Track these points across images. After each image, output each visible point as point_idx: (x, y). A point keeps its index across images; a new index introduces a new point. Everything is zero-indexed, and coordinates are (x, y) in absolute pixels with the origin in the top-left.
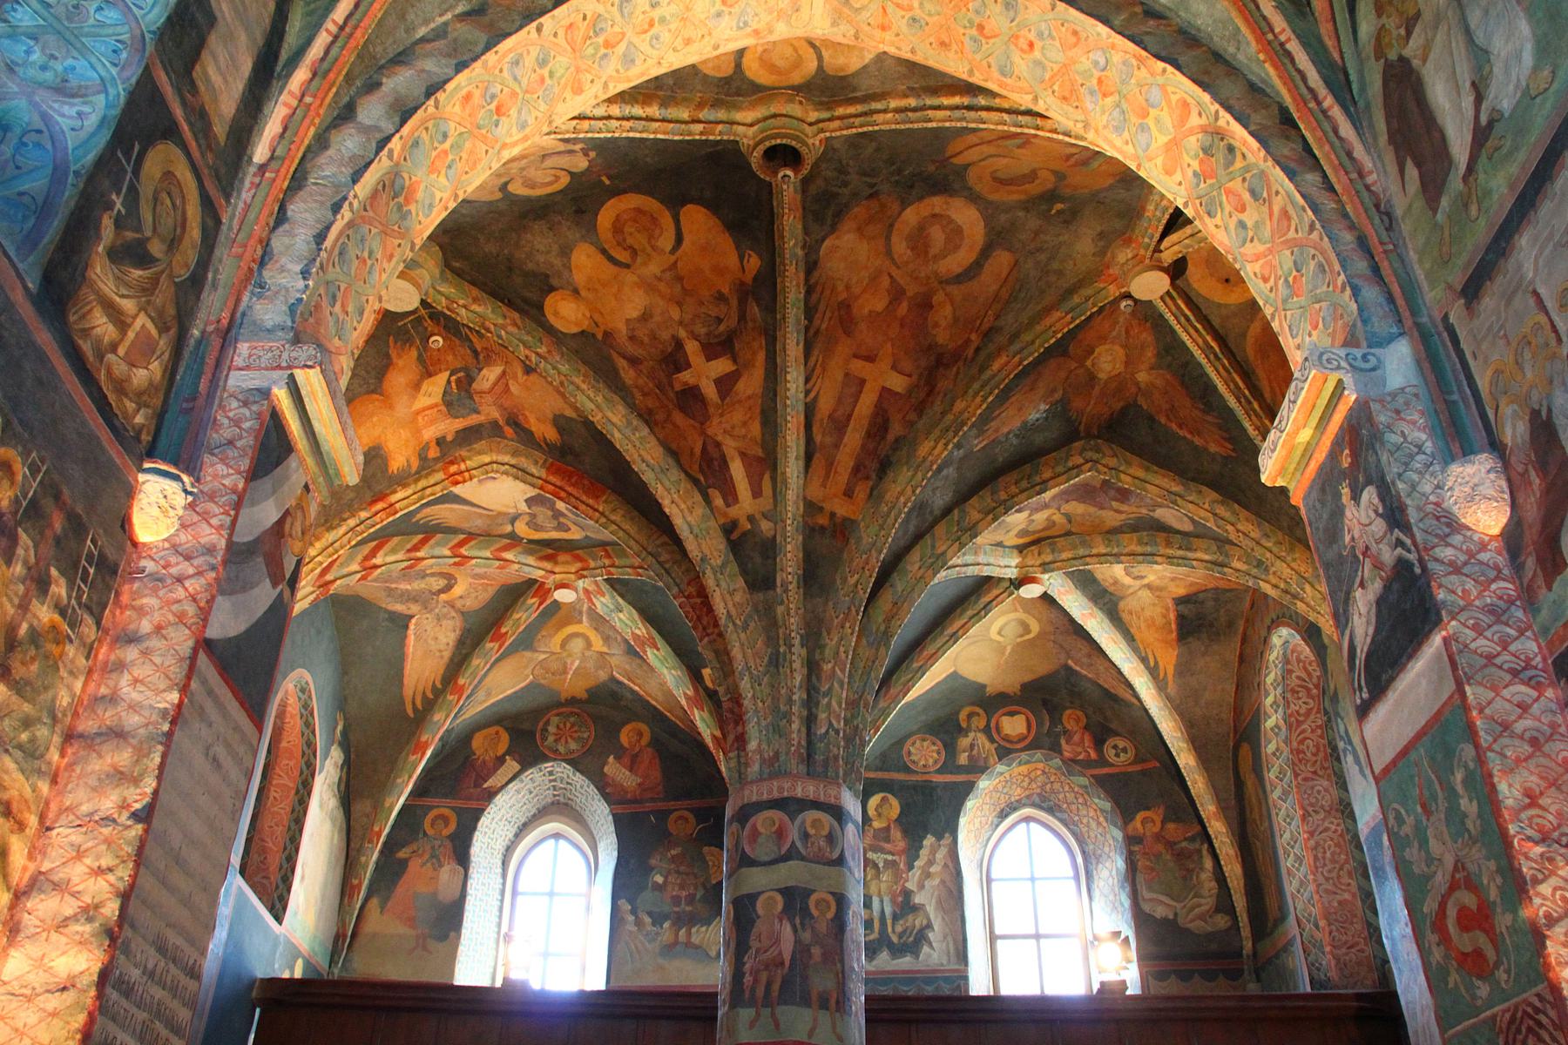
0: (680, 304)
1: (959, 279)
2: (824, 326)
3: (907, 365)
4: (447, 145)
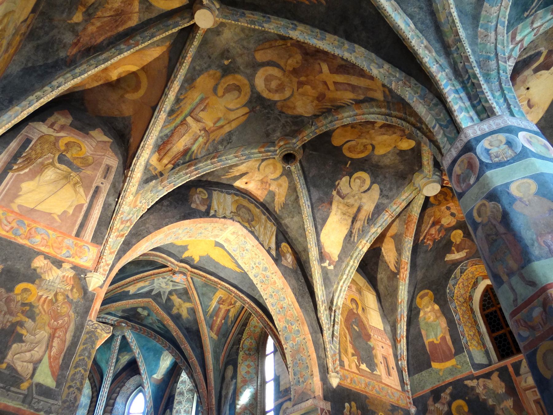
0: (368, 132)
1: (278, 66)
2: (329, 104)
3: (317, 67)
4: (287, 326)
